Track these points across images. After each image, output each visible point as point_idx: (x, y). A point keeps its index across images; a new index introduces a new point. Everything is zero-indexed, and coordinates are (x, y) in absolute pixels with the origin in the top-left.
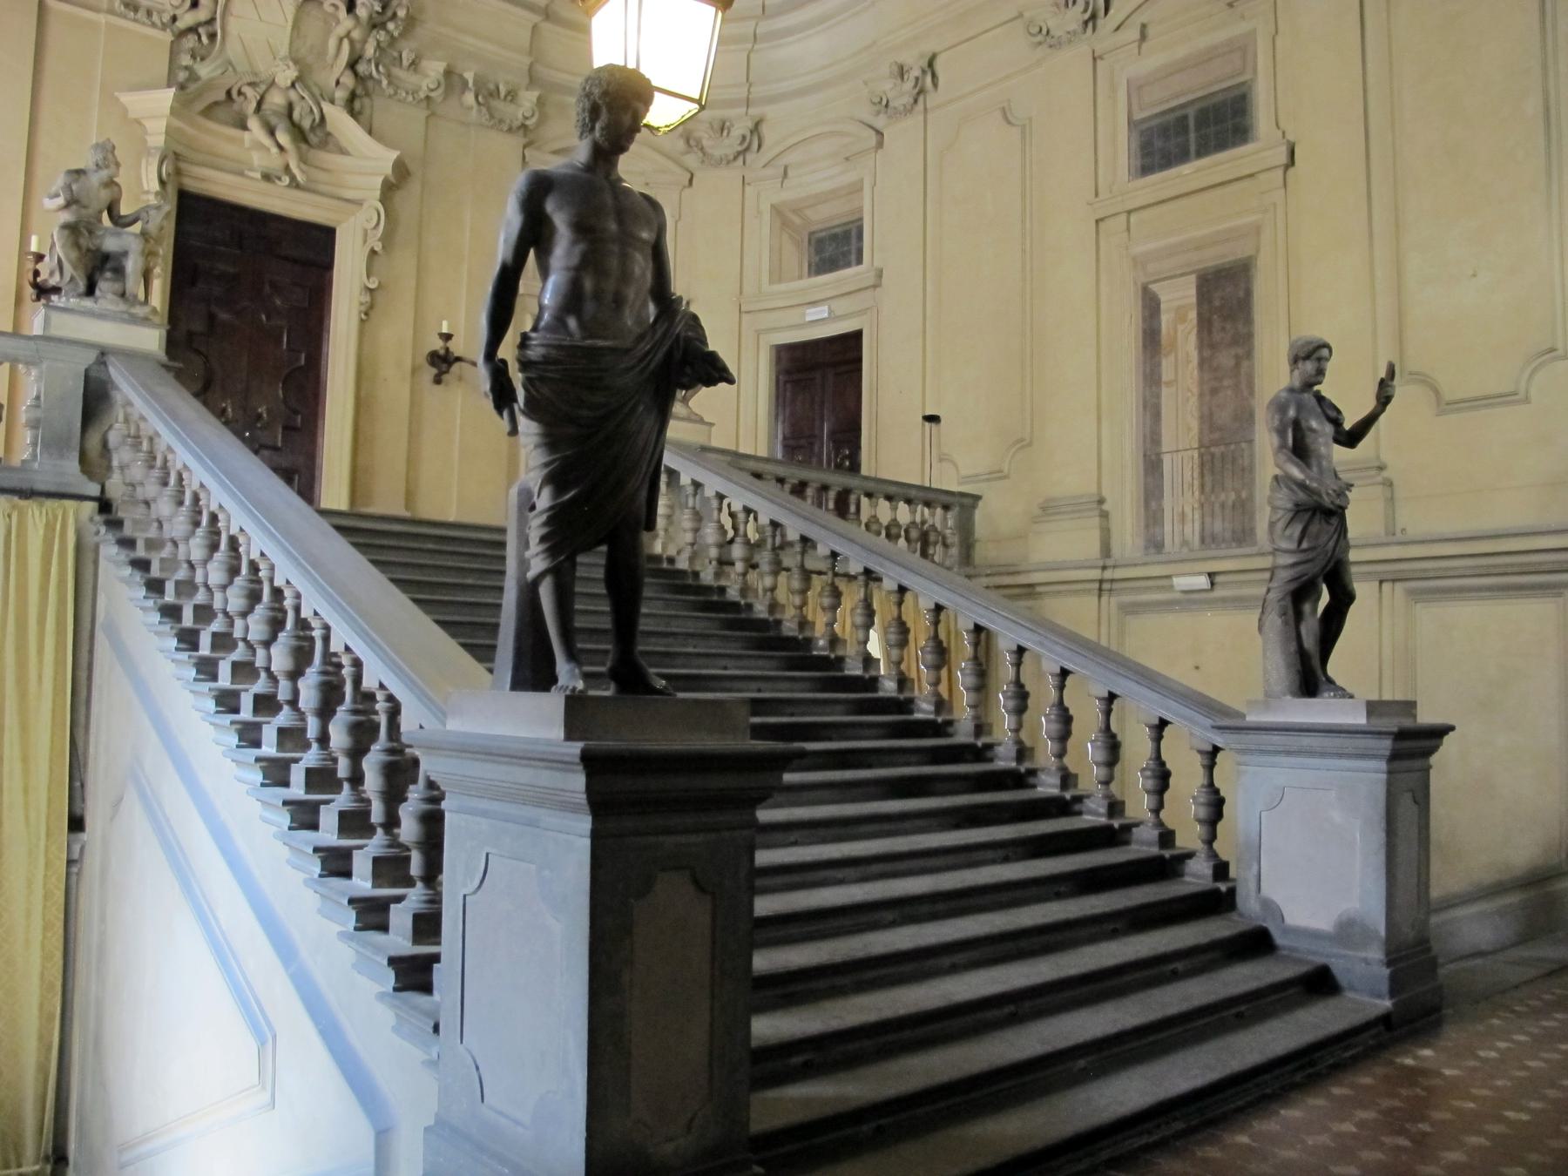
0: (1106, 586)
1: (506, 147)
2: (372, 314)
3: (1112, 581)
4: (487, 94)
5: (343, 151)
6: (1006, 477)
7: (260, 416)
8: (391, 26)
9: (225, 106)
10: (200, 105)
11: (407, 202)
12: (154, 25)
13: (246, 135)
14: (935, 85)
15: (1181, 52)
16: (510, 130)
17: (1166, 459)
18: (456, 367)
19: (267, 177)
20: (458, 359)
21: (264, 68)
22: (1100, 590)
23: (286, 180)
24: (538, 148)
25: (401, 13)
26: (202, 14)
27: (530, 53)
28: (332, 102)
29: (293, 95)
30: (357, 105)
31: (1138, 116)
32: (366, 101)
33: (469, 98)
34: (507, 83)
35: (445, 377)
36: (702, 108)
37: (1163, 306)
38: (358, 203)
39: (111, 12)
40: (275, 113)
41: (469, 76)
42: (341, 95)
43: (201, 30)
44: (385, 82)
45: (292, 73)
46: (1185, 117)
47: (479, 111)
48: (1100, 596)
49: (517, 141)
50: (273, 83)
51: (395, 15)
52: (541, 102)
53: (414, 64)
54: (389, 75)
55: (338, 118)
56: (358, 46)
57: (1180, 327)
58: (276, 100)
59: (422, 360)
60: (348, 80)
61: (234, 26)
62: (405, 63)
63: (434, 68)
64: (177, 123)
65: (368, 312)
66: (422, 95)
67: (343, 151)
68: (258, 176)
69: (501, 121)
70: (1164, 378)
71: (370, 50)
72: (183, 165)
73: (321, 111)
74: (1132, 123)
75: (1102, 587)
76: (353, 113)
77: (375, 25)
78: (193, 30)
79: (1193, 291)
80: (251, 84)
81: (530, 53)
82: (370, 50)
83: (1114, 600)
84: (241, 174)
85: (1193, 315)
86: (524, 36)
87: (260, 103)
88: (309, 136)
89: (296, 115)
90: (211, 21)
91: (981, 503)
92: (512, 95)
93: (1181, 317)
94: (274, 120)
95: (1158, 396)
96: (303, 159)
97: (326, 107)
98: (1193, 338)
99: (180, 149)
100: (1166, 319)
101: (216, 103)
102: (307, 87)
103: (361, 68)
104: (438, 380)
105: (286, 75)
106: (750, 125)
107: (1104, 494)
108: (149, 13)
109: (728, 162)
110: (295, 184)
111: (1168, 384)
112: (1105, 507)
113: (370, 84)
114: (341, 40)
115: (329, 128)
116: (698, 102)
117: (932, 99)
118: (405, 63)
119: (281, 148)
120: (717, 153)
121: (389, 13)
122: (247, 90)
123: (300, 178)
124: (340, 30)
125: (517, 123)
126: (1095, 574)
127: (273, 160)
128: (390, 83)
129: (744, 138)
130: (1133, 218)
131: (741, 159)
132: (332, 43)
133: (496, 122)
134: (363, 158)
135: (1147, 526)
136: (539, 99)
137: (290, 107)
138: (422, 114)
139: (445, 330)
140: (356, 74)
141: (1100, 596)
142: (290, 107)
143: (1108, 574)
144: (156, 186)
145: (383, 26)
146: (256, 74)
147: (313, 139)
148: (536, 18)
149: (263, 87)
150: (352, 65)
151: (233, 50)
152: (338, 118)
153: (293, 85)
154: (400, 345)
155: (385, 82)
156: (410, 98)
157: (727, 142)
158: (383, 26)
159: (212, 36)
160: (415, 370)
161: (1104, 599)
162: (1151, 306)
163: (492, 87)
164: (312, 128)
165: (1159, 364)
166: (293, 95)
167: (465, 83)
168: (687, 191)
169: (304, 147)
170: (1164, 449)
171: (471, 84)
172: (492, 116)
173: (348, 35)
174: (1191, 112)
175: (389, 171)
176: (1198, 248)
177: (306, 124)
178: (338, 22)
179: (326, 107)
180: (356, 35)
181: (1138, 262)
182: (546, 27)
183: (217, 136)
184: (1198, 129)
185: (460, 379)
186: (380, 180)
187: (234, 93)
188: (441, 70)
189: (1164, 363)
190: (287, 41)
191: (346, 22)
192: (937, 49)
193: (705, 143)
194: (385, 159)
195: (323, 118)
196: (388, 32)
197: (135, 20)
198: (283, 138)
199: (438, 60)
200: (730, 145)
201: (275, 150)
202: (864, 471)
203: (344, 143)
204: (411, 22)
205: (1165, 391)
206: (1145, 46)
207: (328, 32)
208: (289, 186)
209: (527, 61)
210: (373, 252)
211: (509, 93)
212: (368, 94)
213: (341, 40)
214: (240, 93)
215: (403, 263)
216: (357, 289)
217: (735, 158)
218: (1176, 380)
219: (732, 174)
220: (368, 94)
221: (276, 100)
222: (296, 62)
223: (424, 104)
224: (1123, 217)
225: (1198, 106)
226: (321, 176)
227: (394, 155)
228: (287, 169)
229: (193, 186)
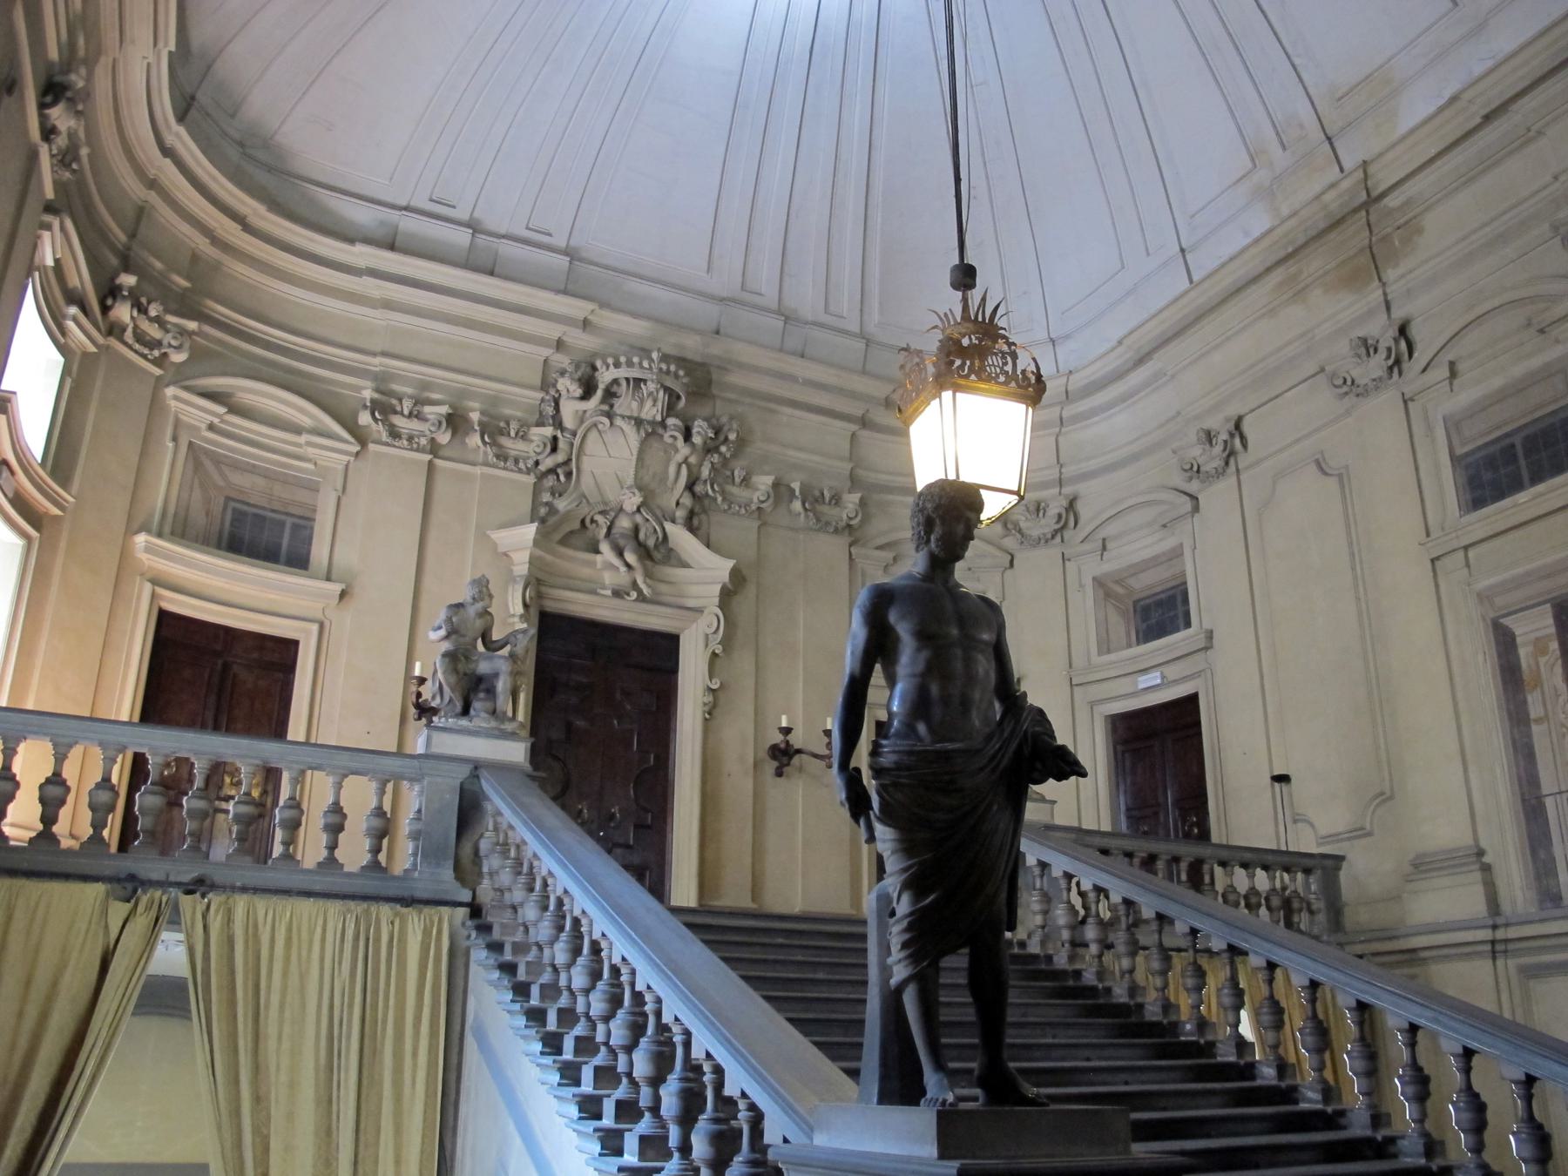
0: (1499, 947)
1: (832, 548)
2: (716, 713)
3: (1506, 941)
4: (812, 499)
5: (685, 565)
6: (1369, 834)
7: (612, 817)
8: (723, 449)
9: (580, 535)
10: (558, 536)
11: (744, 605)
12: (520, 471)
13: (598, 558)
14: (1245, 445)
15: (1497, 382)
16: (836, 531)
17: (1549, 803)
18: (796, 760)
19: (617, 594)
20: (799, 751)
21: (612, 495)
22: (1494, 952)
23: (634, 595)
24: (863, 545)
25: (732, 437)
26: (560, 457)
27: (851, 459)
28: (673, 521)
29: (638, 519)
30: (695, 522)
31: (1460, 451)
32: (703, 517)
33: (797, 505)
34: (831, 488)
35: (785, 769)
36: (1022, 498)
37: (1519, 640)
38: (699, 610)
39: (486, 464)
40: (623, 535)
41: (796, 486)
42: (680, 514)
43: (559, 471)
44: (720, 499)
45: (638, 499)
46: (1513, 446)
47: (807, 517)
48: (1494, 959)
49: (843, 541)
50: (621, 509)
51: (726, 439)
52: (863, 503)
53: (746, 481)
54: (723, 492)
55: (680, 537)
56: (695, 470)
57: (1542, 660)
58: (624, 523)
59: (763, 754)
60: (687, 501)
61: (586, 463)
62: (737, 480)
63: (764, 482)
64: (539, 552)
65: (711, 713)
66: (754, 507)
67: (685, 565)
68: (609, 593)
69: (828, 524)
70: (1533, 715)
71: (705, 472)
72: (543, 589)
73: (664, 529)
74: (1454, 459)
75: (1496, 949)
76: (692, 530)
77: (709, 449)
78: (552, 471)
79: (1551, 621)
80: (602, 513)
81: (851, 459)
82: (705, 472)
83: (1511, 962)
84: (593, 592)
85: (1554, 645)
86: (845, 446)
87: (610, 528)
88: (655, 554)
89: (642, 536)
90: (568, 462)
91: (1345, 864)
92: (836, 500)
93: (1540, 647)
94: (622, 542)
95: (1529, 736)
96: (648, 575)
97: (668, 526)
98: (1559, 669)
99: (540, 575)
100: (1523, 653)
101: (572, 532)
103: (698, 488)
104: (779, 773)
105: (632, 501)
106: (1065, 503)
107: (1484, 844)
108: (516, 461)
110: (642, 598)
111: (1539, 721)
112: (1486, 859)
113: (706, 502)
114: (680, 466)
115: (671, 545)
116: (1017, 493)
117: (1243, 460)
119: (628, 566)
120: (1035, 533)
121: (722, 438)
122: (599, 518)
123: (646, 591)
124: (679, 457)
125: (843, 524)
126: (1486, 934)
127: (621, 577)
128: (724, 499)
129: (1060, 516)
130: (1471, 554)
131: (1058, 539)
132: (672, 470)
133: (823, 525)
134: (704, 570)
135: (1538, 877)
136: (861, 499)
137: (636, 529)
139: (784, 724)
140: (694, 494)
141: (1494, 959)
142: (636, 529)
143: (1500, 934)
144: (520, 610)
145: (716, 450)
146: (605, 503)
147: (657, 555)
148: (854, 427)
150: (690, 487)
151: (587, 483)
152: (680, 537)
153: (638, 510)
154: (741, 743)
155: (720, 499)
157: (1043, 522)
158: (716, 450)
159: (569, 475)
160: (757, 765)
161: (1500, 962)
162: (1505, 642)
163: (817, 493)
164: (656, 546)
165: (1525, 702)
167: (793, 491)
168: (1009, 572)
169: (649, 563)
170: (1545, 790)
172: (818, 520)
173: (686, 461)
174: (1517, 440)
175: (727, 579)
176: (1549, 576)
177: (651, 543)
178: (677, 451)
179: (668, 526)
180: (693, 460)
181: (1483, 597)
182: (864, 434)
183: (575, 562)
184: (1526, 456)
185: (800, 769)
186: (718, 588)
187: (588, 521)
189: (1529, 699)
190: (632, 472)
191: (684, 450)
192: (1242, 412)
193: (1023, 525)
194: (721, 568)
196: (721, 454)
197: (505, 469)
198: (630, 557)
199: (768, 474)
200: (1047, 524)
201: (623, 569)
202: (1215, 839)
203: (685, 557)
204: (742, 442)
205: (1535, 728)
206: (1456, 382)
207: (668, 461)
209: (848, 466)
210: (714, 655)
211: (832, 498)
212: (705, 511)
213: (680, 466)
214: (592, 521)
215: (743, 663)
216: (700, 691)
217: (1053, 537)
218: (1547, 715)
219: (1053, 552)
220: (705, 511)
222: (640, 489)
223: (756, 515)
224: (1461, 554)
225: (1523, 434)
226: (663, 588)
227: (730, 563)
228: (635, 585)
229: (551, 606)
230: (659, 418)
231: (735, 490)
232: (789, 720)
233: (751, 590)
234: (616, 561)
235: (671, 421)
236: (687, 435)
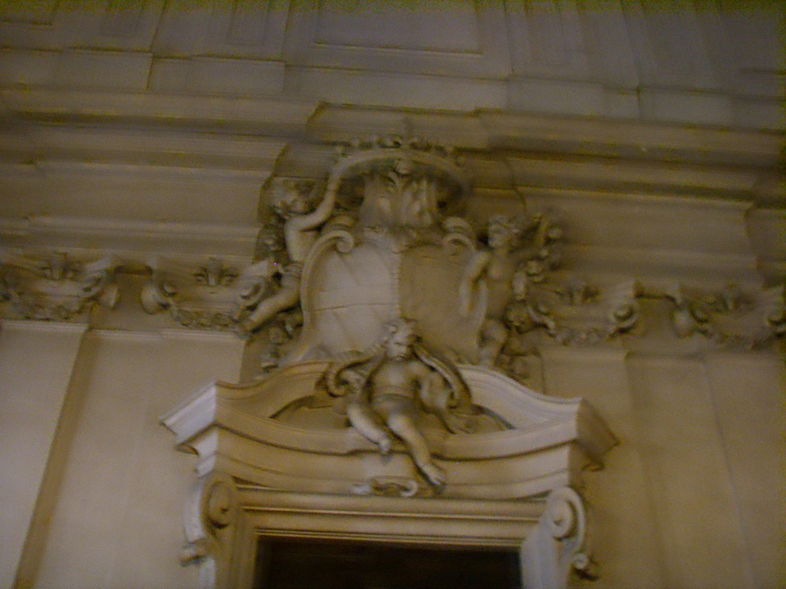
26: (282, 300)
58: (393, 379)
66: (612, 329)
80: (353, 366)
102: (433, 352)
140: (507, 324)
142: (416, 384)
144: (196, 530)
149: (370, 367)
159: (299, 325)
166: (416, 368)
173: (485, 271)
179: (468, 373)
187: (331, 383)
195: (466, 389)
208: (417, 496)
221: (393, 379)
230: (428, 220)
234: (374, 433)
235: (452, 222)
236: (483, 240)
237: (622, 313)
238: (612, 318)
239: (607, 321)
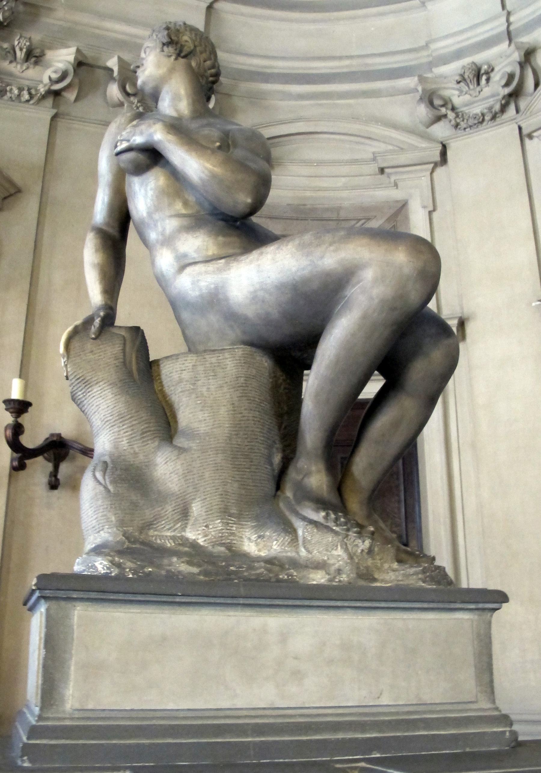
33: (114, 91)
41: (113, 63)
53: (34, 56)
63: (62, 58)
66: (42, 90)
106: (517, 56)
109: (494, 118)
118: (20, 55)
129: (511, 77)
131: (512, 107)
138: (44, 113)
139: (16, 394)
156: (26, 96)
157: (487, 91)
167: (111, 70)
168: (440, 171)
171: (116, 74)
188: (71, 58)
193: (457, 101)
200: (495, 89)
217: (504, 108)
219: (505, 131)
231: (15, 68)
232: (26, 389)
233: (29, 206)
237: (55, 76)
238: (46, 80)
239: (41, 82)
